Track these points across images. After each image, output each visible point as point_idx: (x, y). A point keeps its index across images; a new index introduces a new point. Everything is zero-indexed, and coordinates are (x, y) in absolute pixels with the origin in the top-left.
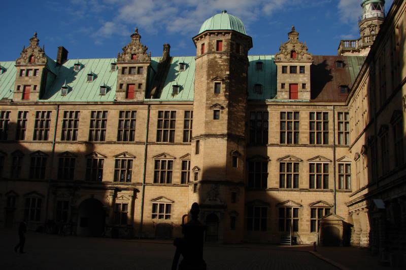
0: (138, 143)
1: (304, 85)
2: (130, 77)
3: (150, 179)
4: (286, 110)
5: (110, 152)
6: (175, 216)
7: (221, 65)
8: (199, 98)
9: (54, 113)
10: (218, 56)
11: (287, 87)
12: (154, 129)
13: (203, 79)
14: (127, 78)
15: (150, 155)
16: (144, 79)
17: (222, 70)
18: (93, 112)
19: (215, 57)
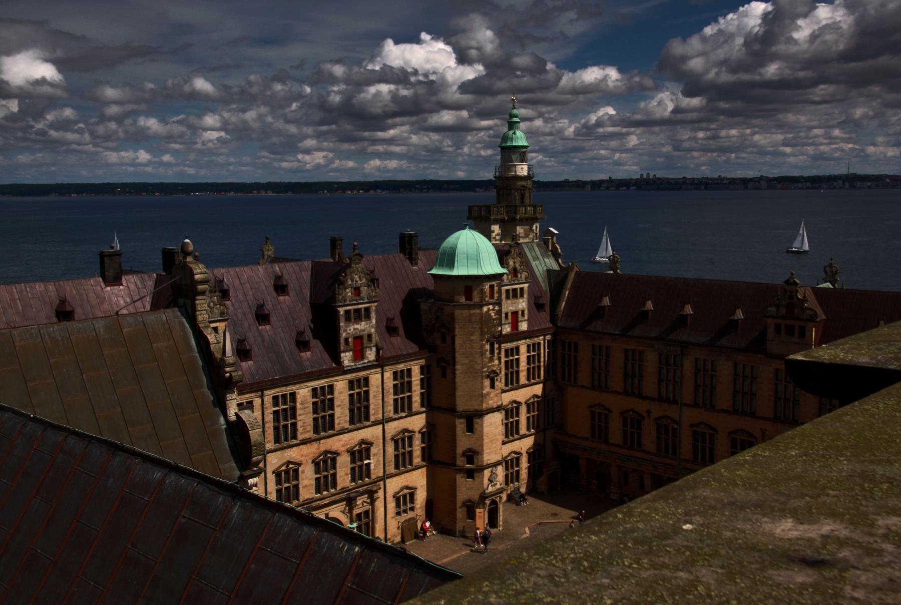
0: (375, 423)
1: (523, 311)
2: (356, 326)
3: (391, 469)
4: (509, 345)
5: (343, 446)
6: (418, 506)
7: (494, 319)
8: (467, 361)
9: (257, 402)
10: (491, 307)
11: (510, 315)
12: (390, 399)
13: (472, 338)
14: (352, 328)
15: (388, 436)
16: (372, 327)
17: (495, 326)
18: (314, 390)
19: (489, 309)
